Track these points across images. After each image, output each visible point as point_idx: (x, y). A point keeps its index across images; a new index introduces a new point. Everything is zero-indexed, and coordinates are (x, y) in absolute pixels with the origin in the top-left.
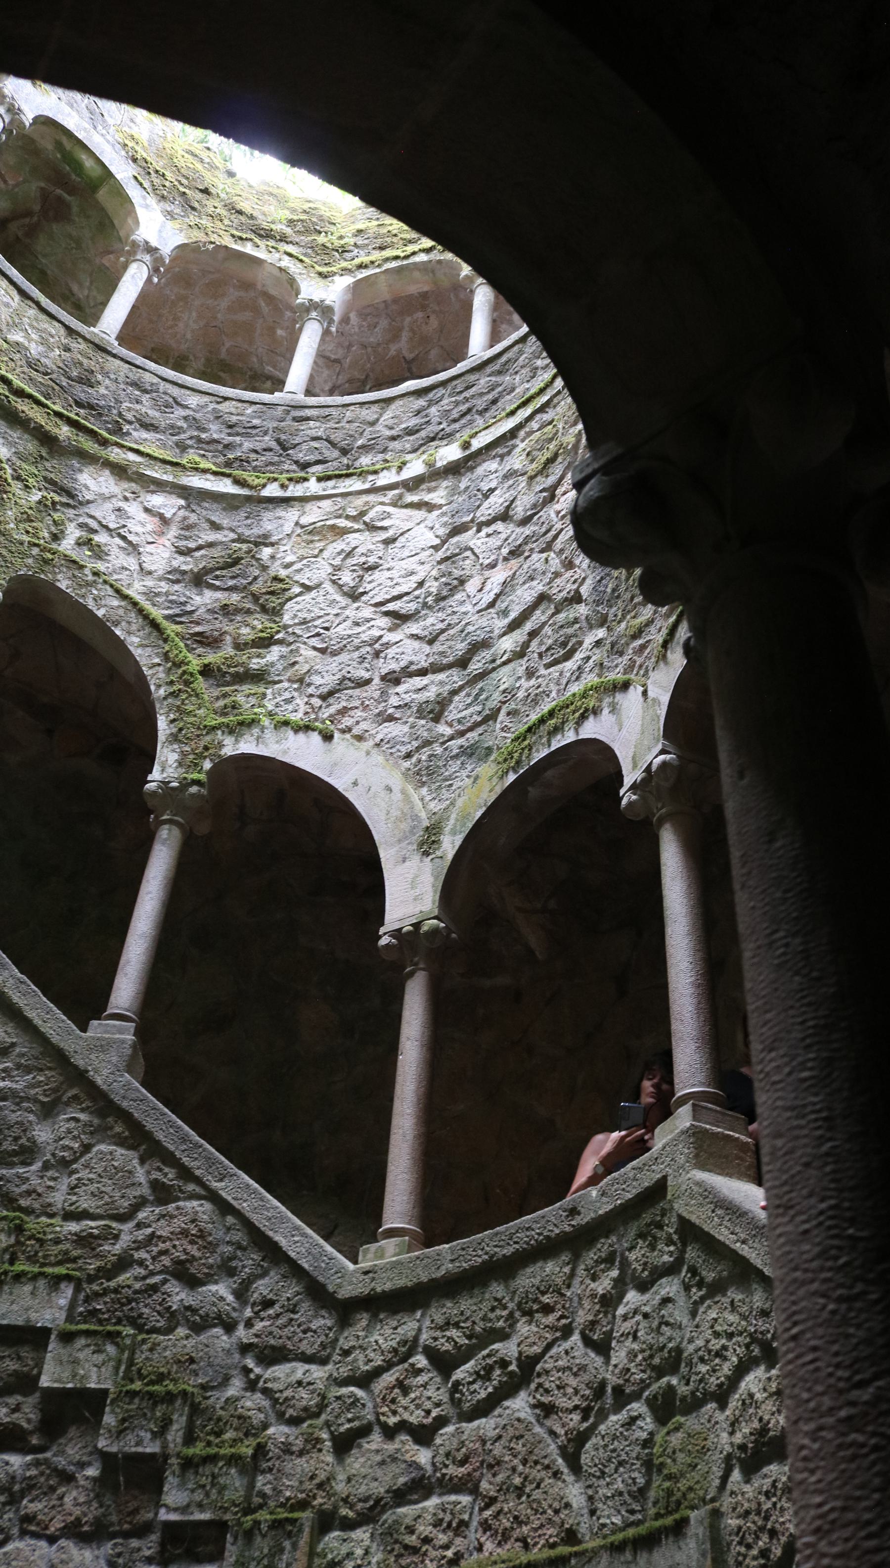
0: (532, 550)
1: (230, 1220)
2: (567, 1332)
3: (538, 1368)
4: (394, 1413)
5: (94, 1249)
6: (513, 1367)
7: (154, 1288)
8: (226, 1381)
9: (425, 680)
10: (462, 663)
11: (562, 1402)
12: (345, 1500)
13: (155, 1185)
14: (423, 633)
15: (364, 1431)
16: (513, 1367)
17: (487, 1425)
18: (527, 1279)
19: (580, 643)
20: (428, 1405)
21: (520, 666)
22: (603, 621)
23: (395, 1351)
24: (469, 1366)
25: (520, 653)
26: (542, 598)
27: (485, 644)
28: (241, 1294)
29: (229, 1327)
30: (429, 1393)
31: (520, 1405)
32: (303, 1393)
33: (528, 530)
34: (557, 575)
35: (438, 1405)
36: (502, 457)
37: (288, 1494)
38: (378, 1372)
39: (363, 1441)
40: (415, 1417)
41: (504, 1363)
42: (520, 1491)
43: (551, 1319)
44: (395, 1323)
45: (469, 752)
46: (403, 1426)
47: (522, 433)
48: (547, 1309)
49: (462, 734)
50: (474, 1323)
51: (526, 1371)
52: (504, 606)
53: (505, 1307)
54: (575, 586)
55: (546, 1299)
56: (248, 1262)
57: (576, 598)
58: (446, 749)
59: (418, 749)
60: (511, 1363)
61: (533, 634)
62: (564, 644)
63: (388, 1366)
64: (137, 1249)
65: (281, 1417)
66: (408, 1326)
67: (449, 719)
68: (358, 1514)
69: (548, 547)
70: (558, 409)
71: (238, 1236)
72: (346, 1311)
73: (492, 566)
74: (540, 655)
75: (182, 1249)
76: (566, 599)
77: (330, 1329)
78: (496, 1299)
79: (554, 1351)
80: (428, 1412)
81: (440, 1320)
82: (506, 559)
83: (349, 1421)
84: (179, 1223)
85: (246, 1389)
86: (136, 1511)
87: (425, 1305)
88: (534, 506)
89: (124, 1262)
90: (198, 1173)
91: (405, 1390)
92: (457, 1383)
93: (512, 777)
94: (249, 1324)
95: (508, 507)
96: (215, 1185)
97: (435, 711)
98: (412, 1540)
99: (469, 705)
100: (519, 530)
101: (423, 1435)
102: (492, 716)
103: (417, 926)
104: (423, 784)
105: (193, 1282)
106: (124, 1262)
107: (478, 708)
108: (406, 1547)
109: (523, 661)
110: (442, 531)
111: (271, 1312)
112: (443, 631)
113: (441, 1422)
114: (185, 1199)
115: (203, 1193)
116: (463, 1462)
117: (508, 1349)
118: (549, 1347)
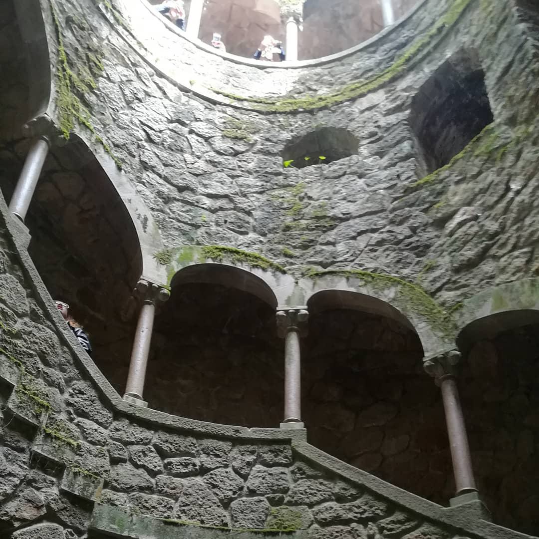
0: (223, 171)
1: (65, 349)
2: (226, 466)
3: (211, 472)
4: (139, 460)
5: (6, 320)
6: (197, 467)
7: (31, 356)
8: (59, 412)
9: (161, 181)
10: (181, 189)
11: (221, 485)
12: (116, 481)
13: (33, 311)
14: (162, 158)
15: (124, 461)
16: (197, 467)
17: (185, 481)
18: (207, 443)
19: (247, 233)
20: (156, 465)
21: (214, 217)
22: (264, 235)
23: (142, 440)
24: (177, 459)
25: (213, 211)
26: (226, 196)
27: (193, 191)
28: (68, 381)
29: (62, 392)
30: (154, 461)
31: (199, 480)
32: (96, 434)
33: (219, 159)
34: (237, 194)
35: (159, 466)
36: (206, 108)
37: (90, 468)
38: (132, 443)
39: (124, 464)
40: (151, 466)
41: (194, 465)
42: (201, 506)
43: (219, 459)
44: (141, 430)
45: (184, 233)
46: (143, 467)
47: (219, 107)
48: (217, 456)
49: (179, 221)
50: (180, 446)
51: (203, 471)
52: (206, 182)
53: (196, 447)
54: (250, 208)
55: (217, 452)
56: (73, 371)
57: (249, 213)
58: (171, 222)
59: (157, 210)
60: (196, 466)
61: (221, 209)
62: (240, 227)
63: (138, 443)
64: (24, 334)
65: (85, 438)
66: (148, 434)
67: (174, 209)
68: (122, 488)
69: (233, 177)
70: (243, 116)
71: (70, 358)
72: (118, 415)
73: (199, 158)
74: (226, 222)
75: (44, 346)
76: (243, 209)
77: (110, 417)
78: (192, 443)
79: (219, 469)
80: (155, 467)
81: (164, 439)
82: (206, 161)
83: (119, 454)
84: (42, 334)
85: (68, 420)
86: (18, 441)
87: (156, 431)
88: (225, 151)
89: (18, 336)
90: (54, 319)
91: (145, 455)
92: (170, 463)
93: (210, 261)
94: (71, 395)
95: (210, 137)
96: (61, 329)
97: (168, 200)
98: (147, 505)
99: (183, 212)
100: (213, 154)
101: (153, 473)
102: (196, 226)
103: (160, 288)
104: (160, 228)
105: (47, 363)
106: (18, 336)
107: (190, 218)
108: (144, 506)
109: (214, 216)
110: (175, 118)
111: (81, 396)
112: (171, 166)
113: (160, 472)
114: (45, 326)
115: (54, 329)
116: (172, 489)
117: (197, 461)
118: (217, 468)
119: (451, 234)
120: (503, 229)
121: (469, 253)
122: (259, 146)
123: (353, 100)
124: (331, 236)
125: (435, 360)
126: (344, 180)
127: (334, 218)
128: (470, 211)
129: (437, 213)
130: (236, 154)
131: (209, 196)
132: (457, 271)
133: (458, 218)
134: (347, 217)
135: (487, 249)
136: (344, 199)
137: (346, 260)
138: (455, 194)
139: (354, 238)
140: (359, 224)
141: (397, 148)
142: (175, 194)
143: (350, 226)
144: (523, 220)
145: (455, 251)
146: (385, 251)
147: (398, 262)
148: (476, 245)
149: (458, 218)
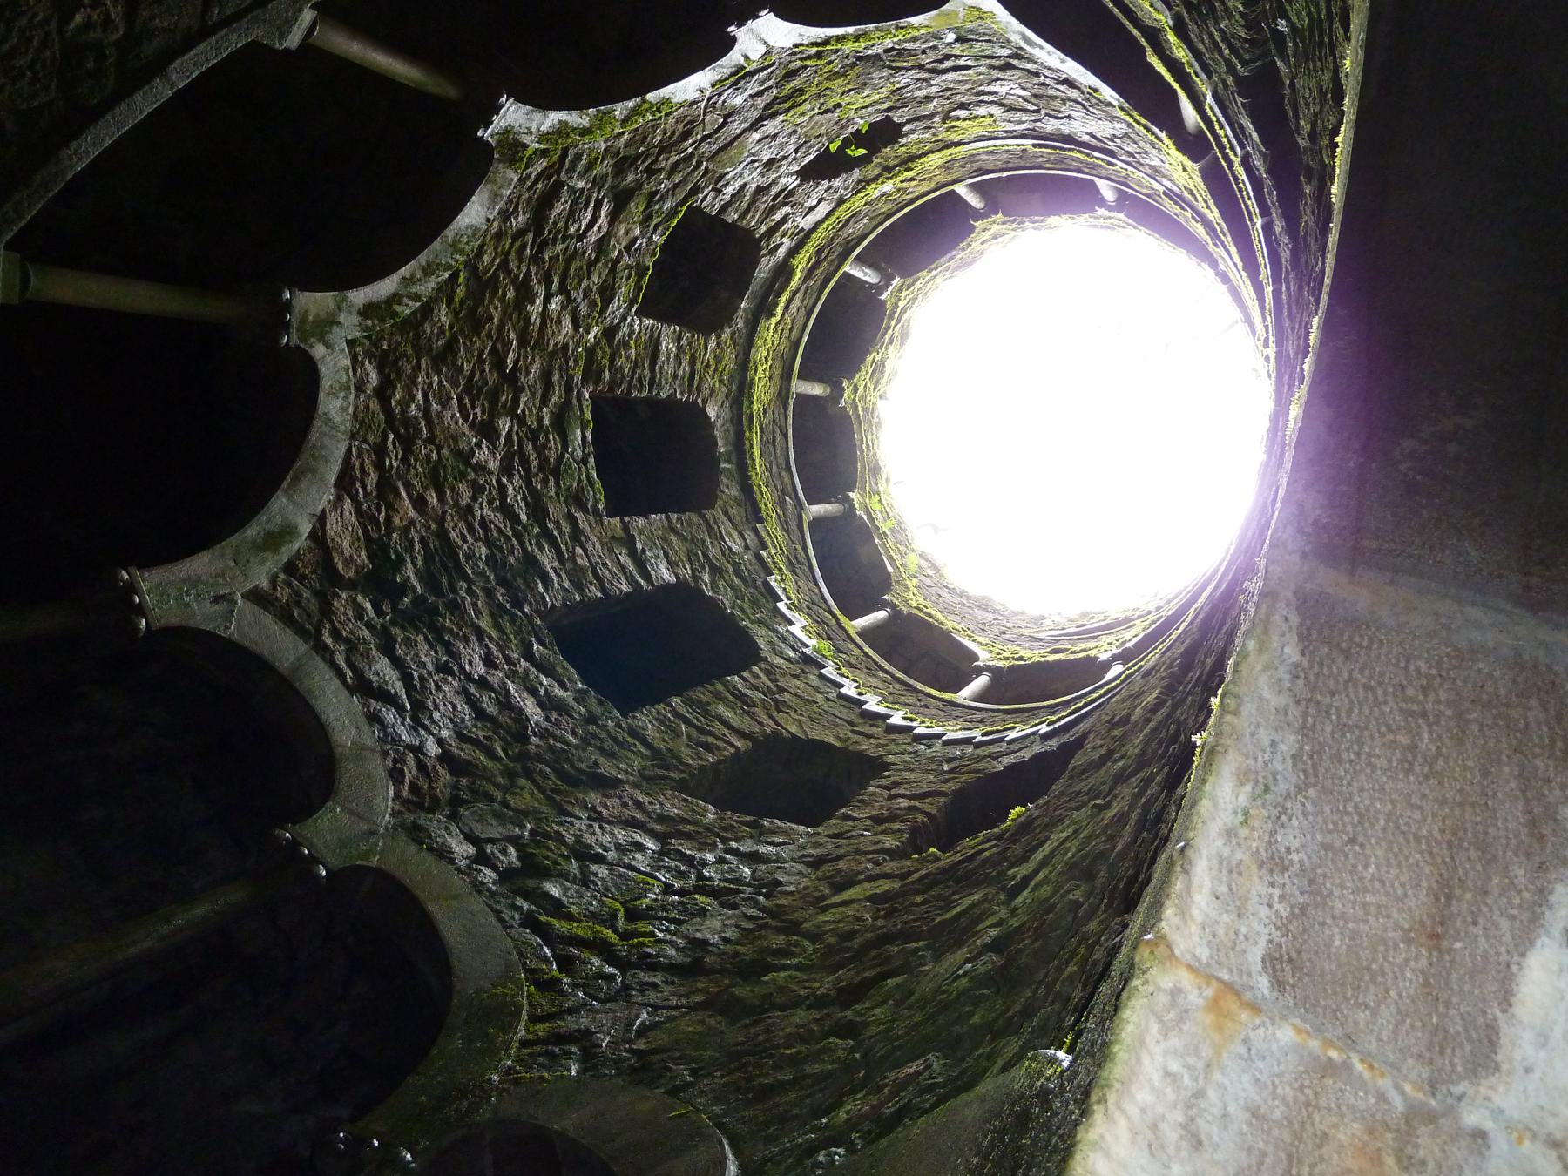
22: (860, 59)
61: (941, 61)
119: (599, 204)
120: (536, 259)
121: (560, 208)
122: (937, 119)
123: (841, 202)
124: (761, 102)
125: (497, 109)
126: (792, 147)
127: (773, 116)
128: (593, 237)
129: (636, 208)
130: (962, 106)
131: (967, 68)
132: (559, 185)
133: (603, 220)
134: (755, 125)
135: (539, 232)
136: (775, 136)
137: (720, 95)
138: (627, 233)
139: (726, 117)
140: (736, 127)
141: (745, 205)
142: (1015, 62)
143: (745, 121)
144: (516, 290)
145: (579, 198)
146: (673, 133)
147: (645, 138)
148: (555, 223)
149: (603, 220)
